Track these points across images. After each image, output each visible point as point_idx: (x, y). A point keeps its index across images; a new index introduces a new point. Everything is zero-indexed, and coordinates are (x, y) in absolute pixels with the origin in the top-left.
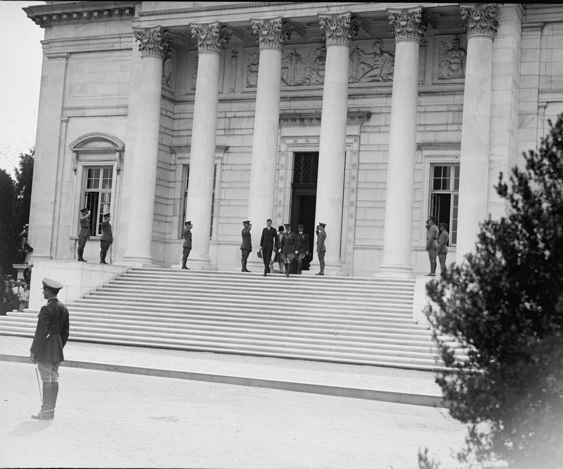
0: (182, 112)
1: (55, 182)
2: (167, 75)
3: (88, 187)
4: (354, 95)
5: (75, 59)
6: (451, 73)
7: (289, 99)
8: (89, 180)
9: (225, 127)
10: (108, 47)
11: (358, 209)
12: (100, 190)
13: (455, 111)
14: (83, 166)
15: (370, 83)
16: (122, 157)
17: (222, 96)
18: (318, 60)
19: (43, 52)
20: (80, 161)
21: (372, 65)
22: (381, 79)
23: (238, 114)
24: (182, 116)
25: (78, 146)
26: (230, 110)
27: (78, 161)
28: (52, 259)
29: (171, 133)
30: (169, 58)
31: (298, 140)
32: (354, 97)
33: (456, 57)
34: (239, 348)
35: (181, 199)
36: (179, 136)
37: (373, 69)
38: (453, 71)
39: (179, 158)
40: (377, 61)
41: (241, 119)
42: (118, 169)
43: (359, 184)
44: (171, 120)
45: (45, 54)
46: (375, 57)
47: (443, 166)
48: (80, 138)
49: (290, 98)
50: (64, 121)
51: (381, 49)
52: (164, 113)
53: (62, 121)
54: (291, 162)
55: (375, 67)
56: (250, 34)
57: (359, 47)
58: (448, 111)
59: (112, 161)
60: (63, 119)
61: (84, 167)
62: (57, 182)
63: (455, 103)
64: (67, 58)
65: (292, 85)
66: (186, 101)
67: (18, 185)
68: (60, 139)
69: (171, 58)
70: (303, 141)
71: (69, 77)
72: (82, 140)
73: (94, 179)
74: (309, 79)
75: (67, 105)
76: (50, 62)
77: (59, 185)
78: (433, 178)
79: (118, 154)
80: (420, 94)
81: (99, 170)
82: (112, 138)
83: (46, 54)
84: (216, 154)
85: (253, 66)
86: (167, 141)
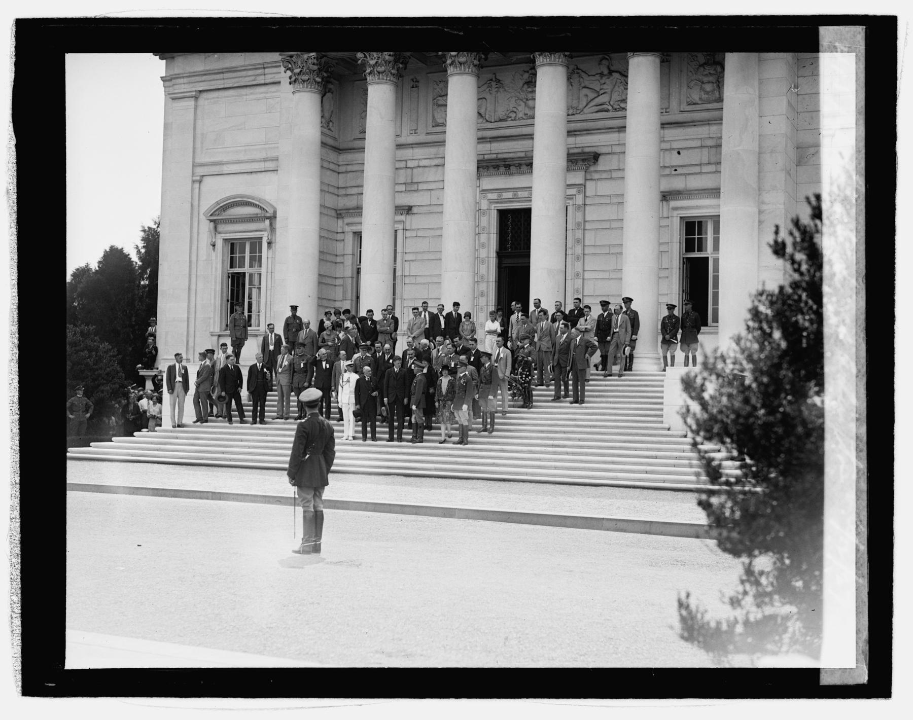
0: (349, 163)
1: (188, 261)
2: (327, 115)
3: (231, 267)
4: (575, 131)
6: (704, 96)
7: (489, 140)
8: (232, 258)
9: (406, 180)
11: (585, 281)
12: (246, 269)
13: (711, 147)
14: (223, 239)
15: (595, 114)
16: (273, 225)
18: (526, 86)
19: (165, 92)
20: (220, 233)
22: (610, 108)
23: (423, 163)
24: (350, 168)
25: (215, 213)
26: (411, 158)
28: (189, 362)
29: (336, 191)
30: (329, 92)
31: (504, 194)
32: (576, 133)
33: (710, 73)
34: (436, 469)
35: (352, 277)
36: (347, 195)
37: (599, 96)
38: (707, 93)
39: (347, 224)
40: (604, 83)
41: (427, 169)
42: (268, 241)
43: (586, 248)
44: (336, 174)
45: (167, 94)
46: (601, 78)
47: (697, 220)
48: (218, 203)
49: (490, 138)
50: (196, 181)
51: (609, 68)
52: (326, 165)
53: (193, 182)
54: (495, 224)
55: (602, 92)
57: (580, 66)
58: (702, 147)
59: (261, 231)
60: (194, 178)
61: (225, 240)
62: (190, 262)
63: (711, 136)
64: (196, 98)
65: (493, 121)
66: (354, 149)
67: (140, 267)
68: (192, 205)
69: (332, 93)
70: (509, 195)
71: (199, 123)
72: (221, 205)
73: (238, 255)
74: (515, 112)
75: (200, 159)
77: (194, 266)
78: (684, 237)
79: (267, 222)
80: (664, 125)
82: (259, 200)
83: (169, 94)
85: (439, 98)
86: (331, 201)
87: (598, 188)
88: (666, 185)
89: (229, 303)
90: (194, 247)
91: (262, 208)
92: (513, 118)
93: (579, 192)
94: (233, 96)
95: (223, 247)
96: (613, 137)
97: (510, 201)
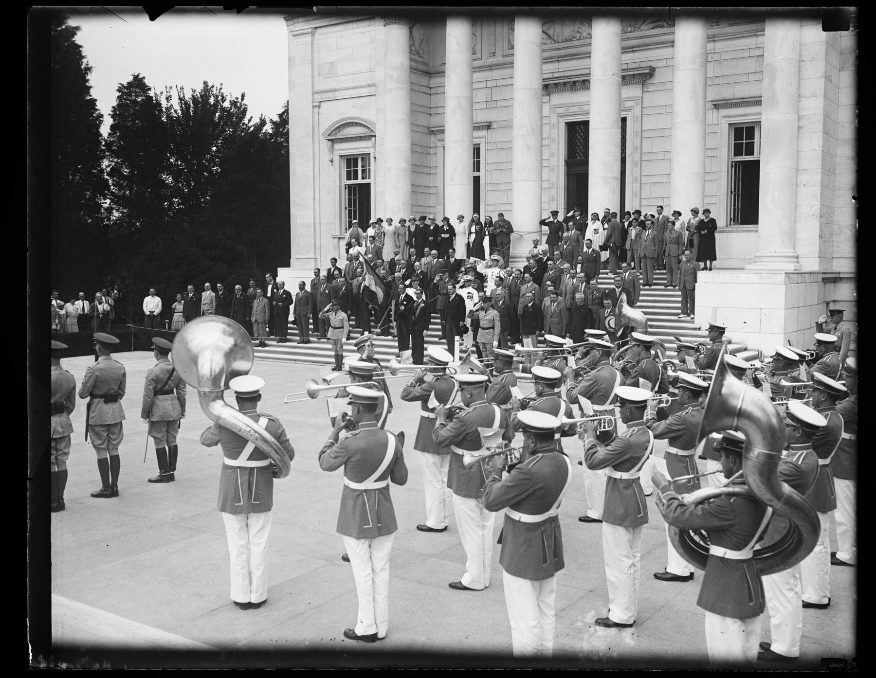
0: (438, 85)
3: (349, 178)
5: (321, 34)
11: (643, 186)
14: (340, 156)
15: (650, 31)
17: (478, 63)
20: (337, 150)
23: (500, 83)
27: (335, 152)
29: (427, 111)
43: (643, 155)
44: (428, 95)
47: (745, 126)
48: (334, 124)
50: (316, 106)
52: (417, 88)
53: (314, 107)
54: (564, 136)
60: (314, 104)
61: (341, 156)
63: (758, 46)
64: (313, 34)
71: (316, 55)
75: (317, 89)
76: (295, 41)
78: (733, 142)
81: (357, 159)
83: (291, 32)
84: (474, 132)
86: (422, 120)
87: (654, 98)
88: (714, 94)
89: (347, 210)
90: (317, 164)
91: (368, 128)
92: (578, 38)
93: (637, 104)
94: (342, 31)
95: (340, 163)
96: (665, 52)
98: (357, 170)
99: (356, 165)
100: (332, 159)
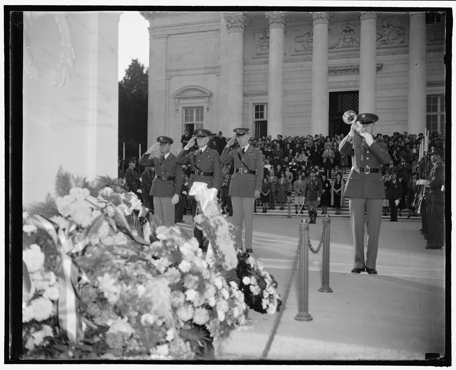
10: (196, 30)
12: (194, 122)
18: (344, 32)
20: (180, 104)
21: (381, 34)
22: (388, 43)
37: (382, 37)
40: (385, 31)
42: (208, 108)
46: (383, 28)
48: (180, 89)
50: (168, 79)
53: (166, 79)
55: (383, 35)
56: (295, 17)
60: (167, 77)
61: (183, 108)
64: (167, 38)
70: (336, 85)
74: (338, 45)
83: (153, 36)
85: (298, 38)
97: (335, 87)
98: (193, 116)
99: (192, 113)
100: (178, 109)
